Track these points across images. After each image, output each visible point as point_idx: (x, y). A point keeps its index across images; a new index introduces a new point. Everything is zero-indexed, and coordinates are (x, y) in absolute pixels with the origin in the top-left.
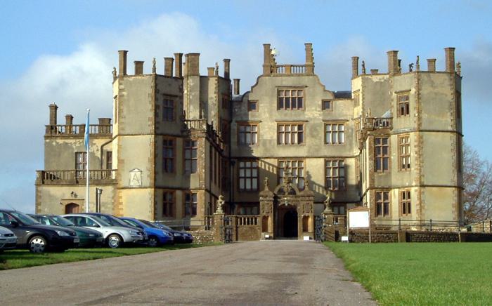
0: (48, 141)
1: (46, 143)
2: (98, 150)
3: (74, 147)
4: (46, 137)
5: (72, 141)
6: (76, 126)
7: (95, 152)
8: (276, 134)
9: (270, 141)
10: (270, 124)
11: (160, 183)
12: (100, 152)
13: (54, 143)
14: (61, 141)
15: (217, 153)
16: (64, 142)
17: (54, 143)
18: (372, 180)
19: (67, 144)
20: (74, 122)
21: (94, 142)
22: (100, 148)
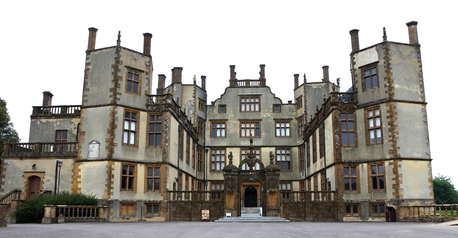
0: (33, 120)
1: (32, 123)
2: (75, 128)
3: (55, 125)
4: (32, 117)
5: (54, 120)
6: (56, 107)
7: (73, 129)
8: (239, 129)
9: (235, 134)
10: (234, 122)
12: (76, 130)
13: (38, 123)
14: (44, 121)
15: (185, 133)
16: (47, 121)
17: (38, 123)
19: (50, 122)
20: (55, 102)
21: (72, 121)
22: (76, 126)
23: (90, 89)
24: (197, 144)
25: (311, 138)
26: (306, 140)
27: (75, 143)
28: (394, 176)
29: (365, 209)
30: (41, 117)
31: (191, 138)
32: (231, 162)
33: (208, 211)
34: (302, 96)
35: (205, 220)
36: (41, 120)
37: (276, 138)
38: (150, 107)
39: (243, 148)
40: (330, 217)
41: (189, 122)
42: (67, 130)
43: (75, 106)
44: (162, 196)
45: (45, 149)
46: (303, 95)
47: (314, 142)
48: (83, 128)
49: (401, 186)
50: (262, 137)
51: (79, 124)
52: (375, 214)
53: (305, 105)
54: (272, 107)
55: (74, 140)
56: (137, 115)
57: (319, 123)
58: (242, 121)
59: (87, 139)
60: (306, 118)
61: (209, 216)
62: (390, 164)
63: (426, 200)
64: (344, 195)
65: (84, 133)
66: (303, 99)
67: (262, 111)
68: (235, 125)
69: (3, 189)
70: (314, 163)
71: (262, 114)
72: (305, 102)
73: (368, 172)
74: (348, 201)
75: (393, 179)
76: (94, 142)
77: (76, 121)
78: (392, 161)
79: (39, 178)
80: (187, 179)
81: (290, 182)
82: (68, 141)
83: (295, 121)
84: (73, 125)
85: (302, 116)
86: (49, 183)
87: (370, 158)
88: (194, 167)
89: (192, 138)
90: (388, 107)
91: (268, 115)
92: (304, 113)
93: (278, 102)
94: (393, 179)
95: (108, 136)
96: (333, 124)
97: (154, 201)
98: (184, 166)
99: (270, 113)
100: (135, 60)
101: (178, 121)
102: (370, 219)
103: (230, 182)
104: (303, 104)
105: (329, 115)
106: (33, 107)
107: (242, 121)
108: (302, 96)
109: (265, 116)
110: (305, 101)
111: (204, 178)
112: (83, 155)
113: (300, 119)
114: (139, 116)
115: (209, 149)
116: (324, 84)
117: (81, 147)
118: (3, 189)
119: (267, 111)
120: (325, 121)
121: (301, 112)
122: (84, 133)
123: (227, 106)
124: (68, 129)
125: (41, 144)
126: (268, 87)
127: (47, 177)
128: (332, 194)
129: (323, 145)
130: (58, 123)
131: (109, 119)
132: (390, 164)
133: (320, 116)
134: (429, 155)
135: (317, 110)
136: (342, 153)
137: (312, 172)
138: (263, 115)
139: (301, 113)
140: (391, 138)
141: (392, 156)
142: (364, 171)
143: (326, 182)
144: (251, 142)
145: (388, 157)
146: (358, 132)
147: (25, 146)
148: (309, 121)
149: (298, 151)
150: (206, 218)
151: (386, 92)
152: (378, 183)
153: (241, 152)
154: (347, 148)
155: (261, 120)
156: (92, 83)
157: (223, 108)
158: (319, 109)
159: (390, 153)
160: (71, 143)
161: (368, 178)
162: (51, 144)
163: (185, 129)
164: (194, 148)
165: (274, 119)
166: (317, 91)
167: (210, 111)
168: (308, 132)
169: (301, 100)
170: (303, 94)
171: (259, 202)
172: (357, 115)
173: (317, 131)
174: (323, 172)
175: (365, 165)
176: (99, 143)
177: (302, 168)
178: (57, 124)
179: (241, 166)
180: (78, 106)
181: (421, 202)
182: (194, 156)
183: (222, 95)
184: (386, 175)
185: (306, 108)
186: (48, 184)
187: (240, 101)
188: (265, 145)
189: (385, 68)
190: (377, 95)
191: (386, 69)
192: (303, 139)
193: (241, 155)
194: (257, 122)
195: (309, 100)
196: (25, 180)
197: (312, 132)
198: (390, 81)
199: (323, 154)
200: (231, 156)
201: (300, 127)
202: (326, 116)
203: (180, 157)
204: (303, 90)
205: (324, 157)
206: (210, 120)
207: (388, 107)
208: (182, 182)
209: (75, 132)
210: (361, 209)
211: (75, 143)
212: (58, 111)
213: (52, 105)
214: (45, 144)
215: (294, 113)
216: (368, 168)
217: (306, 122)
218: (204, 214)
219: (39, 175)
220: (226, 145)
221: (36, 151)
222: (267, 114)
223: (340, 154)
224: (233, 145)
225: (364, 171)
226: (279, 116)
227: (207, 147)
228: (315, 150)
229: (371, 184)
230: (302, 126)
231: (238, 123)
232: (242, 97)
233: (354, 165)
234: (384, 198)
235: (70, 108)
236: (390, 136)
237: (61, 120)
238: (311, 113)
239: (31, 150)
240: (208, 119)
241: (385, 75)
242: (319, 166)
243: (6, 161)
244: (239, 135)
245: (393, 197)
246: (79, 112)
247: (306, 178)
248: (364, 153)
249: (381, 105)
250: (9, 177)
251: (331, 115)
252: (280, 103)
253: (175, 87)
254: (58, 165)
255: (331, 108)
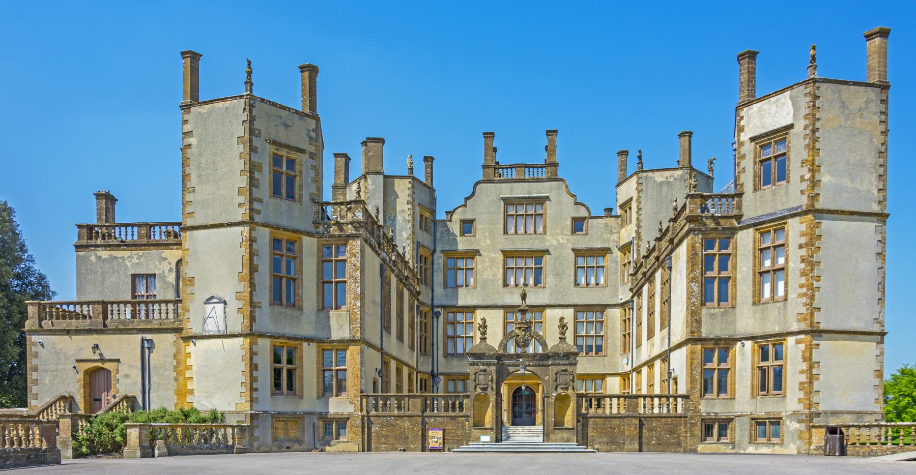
0: (82, 253)
3: (129, 264)
7: (167, 273)
8: (501, 270)
10: (493, 255)
11: (266, 321)
12: (174, 275)
13: (93, 258)
14: (104, 254)
15: (394, 280)
16: (111, 255)
17: (93, 258)
18: (694, 318)
19: (116, 258)
21: (164, 255)
23: (196, 189)
24: (418, 300)
25: (645, 289)
26: (638, 293)
27: (177, 302)
28: (804, 366)
29: (741, 431)
30: (97, 246)
31: (405, 290)
32: (484, 339)
33: (441, 432)
34: (631, 199)
35: (433, 450)
36: (99, 253)
37: (577, 289)
38: (321, 228)
39: (508, 309)
40: (672, 444)
41: (401, 257)
42: (154, 275)
43: (166, 225)
44: (351, 403)
45: (115, 312)
46: (635, 198)
47: (651, 297)
48: (188, 271)
49: (816, 385)
50: (547, 286)
51: (179, 262)
52: (761, 440)
53: (638, 219)
54: (569, 222)
55: (171, 296)
56: (297, 245)
57: (662, 257)
58: (508, 254)
59: (200, 293)
60: (639, 246)
61: (441, 441)
62: (798, 342)
63: (866, 413)
64: (703, 402)
65: (191, 280)
66: (634, 205)
67: (548, 233)
68: (493, 261)
69: (37, 394)
70: (649, 338)
71: (548, 237)
72: (638, 212)
73: (753, 357)
74: (708, 414)
75: (802, 372)
76: (215, 300)
77: (173, 255)
78: (802, 337)
79: (109, 372)
80: (399, 372)
81: (603, 377)
82: (158, 298)
83: (617, 254)
84: (166, 263)
85: (631, 243)
86: (129, 381)
87: (758, 331)
88: (412, 347)
89: (409, 290)
90: (804, 225)
91: (561, 241)
92: (634, 235)
93: (583, 213)
94: (802, 372)
95: (243, 287)
96: (688, 262)
97: (337, 414)
98: (391, 345)
99: (566, 235)
100: (286, 126)
101: (379, 255)
102: (751, 449)
103: (482, 377)
104: (634, 216)
105: (681, 241)
106: (80, 226)
107: (508, 254)
108: (631, 199)
109: (555, 243)
110: (639, 209)
111: (433, 371)
112: (193, 327)
113: (625, 248)
114: (301, 247)
115: (441, 310)
116: (680, 172)
117: (189, 310)
118: (37, 394)
119: (558, 231)
120: (673, 255)
121: (627, 234)
122: (191, 280)
123: (477, 222)
124: (156, 272)
125: (104, 304)
126: (562, 180)
127: (123, 369)
128: (679, 400)
129: (666, 302)
130: (135, 260)
131: (243, 252)
132: (798, 342)
133: (664, 243)
134: (882, 324)
135: (661, 230)
136: (703, 319)
137: (644, 357)
138: (549, 242)
139: (629, 234)
140: (804, 290)
141: (804, 326)
142: (744, 358)
143: (670, 378)
144: (524, 297)
145: (795, 327)
146: (739, 277)
147: (71, 308)
148: (643, 252)
149: (619, 315)
150: (437, 445)
151: (802, 192)
152: (770, 381)
153: (505, 318)
154: (712, 311)
155: (547, 252)
156: (199, 176)
157: (467, 226)
158: (664, 228)
159: (799, 321)
160: (167, 302)
161: (753, 369)
162: (125, 303)
163: (393, 271)
164: (411, 309)
165: (573, 250)
166: (665, 188)
167: (442, 233)
168: (640, 275)
169: (630, 209)
170: (635, 195)
171: (539, 416)
172: (739, 241)
173: (658, 275)
174: (665, 357)
175: (749, 344)
176: (225, 303)
177: (626, 348)
178: (135, 261)
179: (504, 345)
180: (173, 224)
181: (855, 416)
182: (411, 326)
183: (467, 199)
184: (789, 363)
185: (639, 226)
186: (126, 382)
187: (506, 211)
188: (552, 302)
189: (805, 139)
190: (784, 199)
191: (807, 141)
192: (631, 290)
193: (506, 324)
194: (539, 255)
195: (647, 207)
196: (81, 376)
197: (649, 279)
198: (814, 169)
199: (666, 323)
200: (484, 326)
201: (625, 265)
202: (674, 245)
203: (385, 327)
204: (635, 186)
205: (667, 329)
206: (443, 251)
207: (804, 225)
208: (389, 377)
209: (172, 278)
210: (733, 430)
211: (177, 302)
212: (132, 235)
213: (117, 221)
214: (112, 303)
215: (614, 237)
216: (753, 350)
217: (638, 254)
218: (433, 437)
219: (107, 366)
220: (474, 302)
221: (100, 319)
222: (559, 238)
223: (699, 322)
224: (489, 303)
225: (744, 358)
226: (582, 242)
227: (438, 307)
228: (651, 314)
229: (757, 382)
230: (629, 263)
231: (501, 257)
232: (508, 202)
233: (724, 346)
234: (781, 410)
235: (157, 228)
236: (802, 286)
237: (141, 252)
238: (650, 235)
239: (84, 317)
240: (438, 249)
241: (805, 155)
242: (658, 346)
243: (35, 338)
244: (501, 282)
245: (800, 407)
246: (176, 236)
247: (634, 370)
248: (747, 320)
249: (790, 221)
250: (46, 371)
251: (685, 243)
252: (587, 215)
253: (369, 181)
254: (147, 348)
255: (686, 228)
